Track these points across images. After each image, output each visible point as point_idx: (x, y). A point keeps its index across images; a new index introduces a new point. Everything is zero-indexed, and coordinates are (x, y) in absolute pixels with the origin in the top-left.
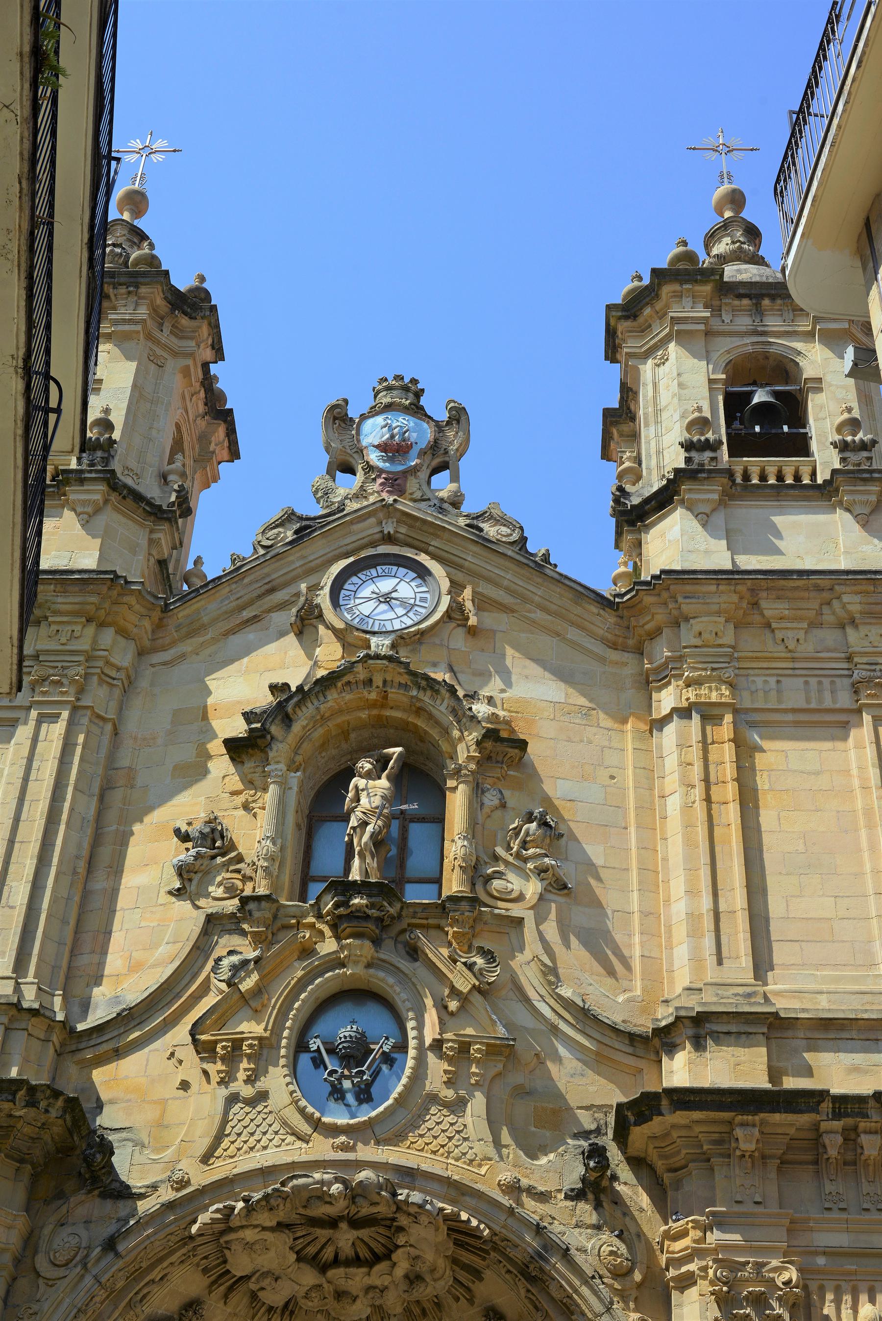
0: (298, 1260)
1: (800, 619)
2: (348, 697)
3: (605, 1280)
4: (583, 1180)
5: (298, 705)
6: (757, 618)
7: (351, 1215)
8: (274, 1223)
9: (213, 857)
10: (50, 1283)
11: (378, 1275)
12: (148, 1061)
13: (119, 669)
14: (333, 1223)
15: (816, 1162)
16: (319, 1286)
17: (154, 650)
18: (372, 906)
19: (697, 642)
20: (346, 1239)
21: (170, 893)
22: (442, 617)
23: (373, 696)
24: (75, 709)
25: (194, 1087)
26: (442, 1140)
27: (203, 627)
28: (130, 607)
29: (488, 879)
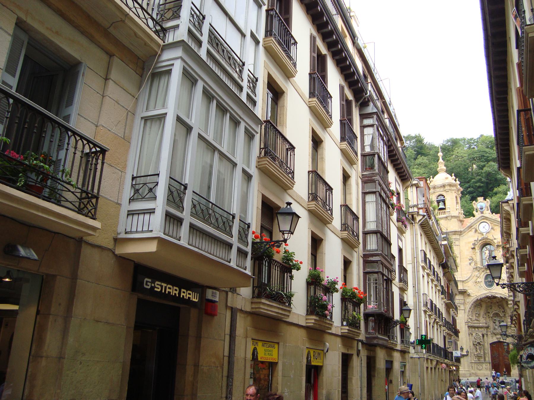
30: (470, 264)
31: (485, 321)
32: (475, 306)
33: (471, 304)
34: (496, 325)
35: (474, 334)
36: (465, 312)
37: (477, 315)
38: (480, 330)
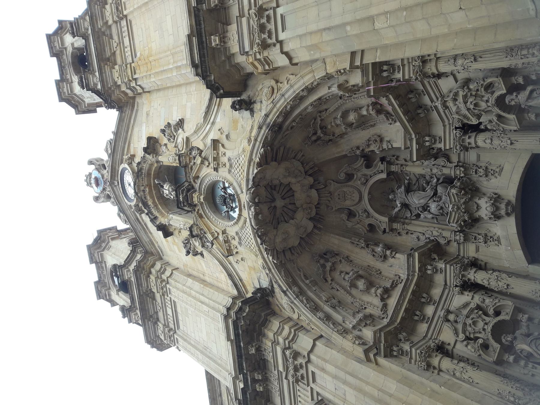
1: (109, 42)
2: (148, 198)
4: (246, 110)
5: (152, 214)
6: (112, 58)
7: (269, 200)
9: (191, 244)
11: (296, 188)
13: (162, 267)
15: (225, 8)
16: (304, 209)
17: (159, 254)
18: (182, 193)
19: (120, 78)
20: (279, 203)
21: (203, 257)
22: (129, 166)
23: (147, 189)
24: (168, 283)
25: (241, 256)
26: (240, 167)
27: (151, 240)
28: (145, 264)
29: (179, 149)
30: (196, 254)
31: (401, 258)
32: (324, 279)
35: (447, 336)
38: (436, 292)
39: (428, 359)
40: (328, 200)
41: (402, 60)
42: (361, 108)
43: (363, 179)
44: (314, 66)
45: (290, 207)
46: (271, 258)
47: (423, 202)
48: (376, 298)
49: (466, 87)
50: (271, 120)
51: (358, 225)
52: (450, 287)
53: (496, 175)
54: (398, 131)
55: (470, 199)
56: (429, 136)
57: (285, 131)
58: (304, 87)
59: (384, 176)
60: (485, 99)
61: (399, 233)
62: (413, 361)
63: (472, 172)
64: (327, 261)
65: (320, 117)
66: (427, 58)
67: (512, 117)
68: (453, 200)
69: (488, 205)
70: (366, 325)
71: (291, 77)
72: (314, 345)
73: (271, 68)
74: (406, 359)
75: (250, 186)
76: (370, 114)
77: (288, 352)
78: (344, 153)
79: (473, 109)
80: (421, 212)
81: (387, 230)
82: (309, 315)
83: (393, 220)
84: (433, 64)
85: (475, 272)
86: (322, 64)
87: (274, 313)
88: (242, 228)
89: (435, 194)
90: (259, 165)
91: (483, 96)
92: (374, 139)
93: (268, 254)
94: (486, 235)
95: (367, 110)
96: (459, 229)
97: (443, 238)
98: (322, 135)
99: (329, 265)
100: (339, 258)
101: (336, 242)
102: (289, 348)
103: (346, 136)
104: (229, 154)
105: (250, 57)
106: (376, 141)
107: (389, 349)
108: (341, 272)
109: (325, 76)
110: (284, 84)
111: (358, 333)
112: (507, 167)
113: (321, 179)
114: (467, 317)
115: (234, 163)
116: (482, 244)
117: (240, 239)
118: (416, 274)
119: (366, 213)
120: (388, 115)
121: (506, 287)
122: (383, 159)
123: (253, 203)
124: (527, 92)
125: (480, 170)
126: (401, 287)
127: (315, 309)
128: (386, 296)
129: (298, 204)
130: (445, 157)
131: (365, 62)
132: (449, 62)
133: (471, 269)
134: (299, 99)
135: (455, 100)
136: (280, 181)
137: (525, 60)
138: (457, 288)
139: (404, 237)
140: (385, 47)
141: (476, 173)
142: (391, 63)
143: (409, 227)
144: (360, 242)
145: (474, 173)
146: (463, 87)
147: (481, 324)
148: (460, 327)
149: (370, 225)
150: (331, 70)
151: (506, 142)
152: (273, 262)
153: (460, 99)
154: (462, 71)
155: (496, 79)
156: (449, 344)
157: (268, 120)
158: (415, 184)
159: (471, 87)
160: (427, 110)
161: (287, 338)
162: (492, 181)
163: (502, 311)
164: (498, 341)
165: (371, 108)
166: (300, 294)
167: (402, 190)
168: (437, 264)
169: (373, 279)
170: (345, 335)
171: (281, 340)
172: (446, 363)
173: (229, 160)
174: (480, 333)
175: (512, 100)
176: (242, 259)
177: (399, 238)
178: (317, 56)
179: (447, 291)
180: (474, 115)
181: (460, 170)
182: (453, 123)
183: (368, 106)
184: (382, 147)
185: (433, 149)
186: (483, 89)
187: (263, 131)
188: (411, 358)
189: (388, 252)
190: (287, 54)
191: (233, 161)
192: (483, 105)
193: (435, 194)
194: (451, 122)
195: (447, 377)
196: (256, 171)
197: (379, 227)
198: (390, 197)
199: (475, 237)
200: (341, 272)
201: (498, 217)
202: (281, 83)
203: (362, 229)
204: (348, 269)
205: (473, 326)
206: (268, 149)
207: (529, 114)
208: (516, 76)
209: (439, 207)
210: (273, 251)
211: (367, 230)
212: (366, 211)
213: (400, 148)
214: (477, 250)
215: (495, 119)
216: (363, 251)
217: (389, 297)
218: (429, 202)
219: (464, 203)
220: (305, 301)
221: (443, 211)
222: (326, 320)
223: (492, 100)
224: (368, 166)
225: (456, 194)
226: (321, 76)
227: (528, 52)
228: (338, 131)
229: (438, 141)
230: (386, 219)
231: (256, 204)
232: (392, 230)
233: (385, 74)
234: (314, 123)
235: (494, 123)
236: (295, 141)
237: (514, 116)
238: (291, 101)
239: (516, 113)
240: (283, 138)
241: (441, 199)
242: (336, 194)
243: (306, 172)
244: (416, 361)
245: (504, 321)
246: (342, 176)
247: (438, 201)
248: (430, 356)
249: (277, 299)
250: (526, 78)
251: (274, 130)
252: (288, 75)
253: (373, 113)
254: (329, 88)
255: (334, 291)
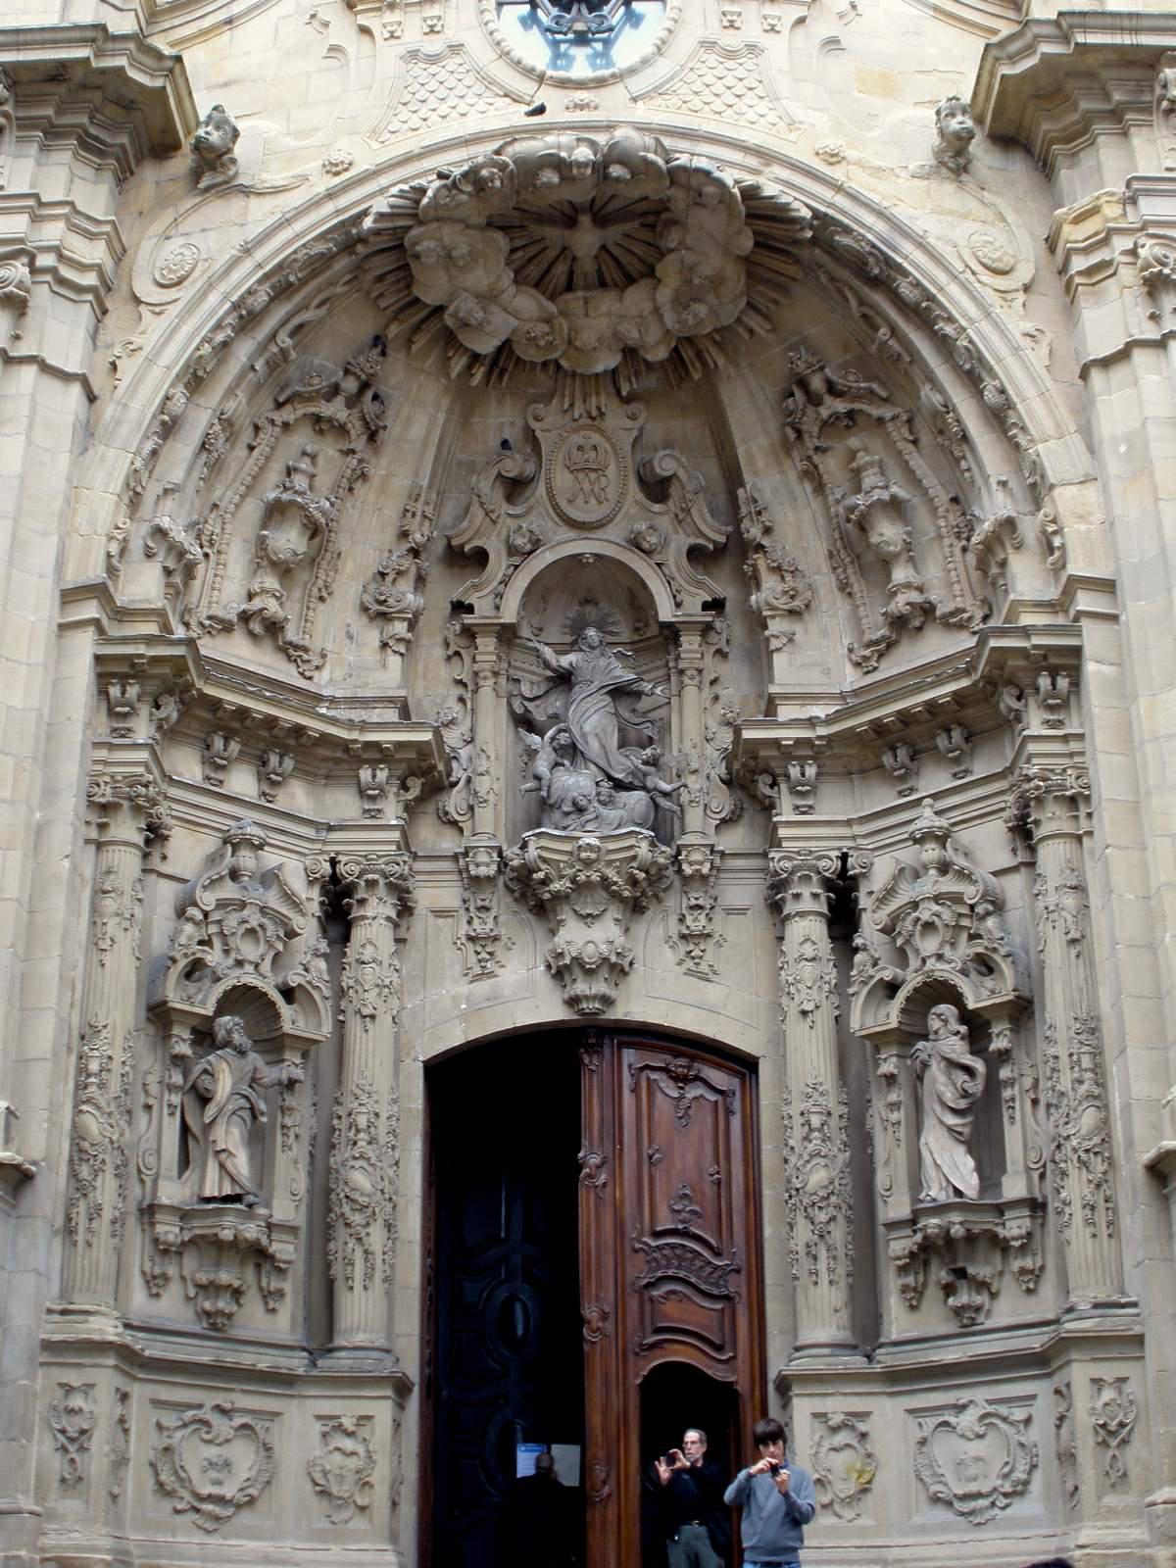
0: (516, 281)
3: (983, 279)
4: (938, 154)
8: (482, 221)
10: (157, 309)
11: (636, 298)
12: (277, 30)
14: (569, 218)
20: (586, 240)
31: (389, 677)
33: (217, 305)
34: (570, 752)
35: (187, 850)
36: (88, 433)
37: (289, 540)
38: (297, 797)
39: (126, 804)
40: (572, 405)
41: (1080, 737)
42: (911, 559)
43: (653, 540)
44: (1076, 441)
45: (561, 269)
46: (381, 205)
47: (593, 748)
48: (244, 593)
49: (991, 908)
50: (906, 258)
51: (481, 514)
52: (324, 842)
53: (690, 964)
54: (827, 672)
55: (616, 896)
56: (818, 774)
57: (856, 294)
58: (1015, 398)
59: (666, 612)
60: (947, 951)
61: (457, 653)
62: (103, 754)
63: (697, 896)
64: (352, 402)
65: (894, 418)
66: (1083, 810)
67: (891, 1015)
68: (611, 846)
69: (604, 948)
70: (168, 572)
71: (1043, 350)
72: (65, 377)
73: (1077, 280)
74: (103, 726)
75: (667, 142)
76: (895, 594)
77: (19, 270)
78: (747, 477)
79: (918, 919)
80: (553, 739)
81: (468, 619)
82: (175, 355)
83: (507, 635)
84: (1067, 827)
85: (388, 919)
86: (1082, 473)
87: (123, 177)
88: (489, 82)
89: (620, 786)
90: (751, 194)
91: (953, 945)
92: (800, 587)
93: (402, 195)
94: (496, 939)
95: (908, 586)
96: (515, 863)
97: (465, 806)
98: (824, 412)
99: (336, 409)
100: (359, 443)
101: (416, 431)
102: (34, 270)
103: (808, 487)
104: (776, 48)
105: (1117, 210)
106: (792, 597)
107: (125, 669)
108: (313, 457)
109: (1043, 476)
110: (1022, 318)
111: (136, 546)
112: (712, 992)
113: (650, 381)
114: (263, 910)
115: (740, 72)
116: (464, 929)
117: (433, 59)
118: (354, 735)
119: (528, 547)
120: (886, 647)
121: (366, 1011)
122: (716, 605)
123: (604, 156)
124: (968, 1060)
125: (702, 918)
126: (287, 673)
127: (195, 379)
128: (256, 627)
129: (574, 300)
130: (733, 812)
131: (1086, 624)
132: (1068, 872)
133: (395, 905)
134: (973, 375)
135: (944, 868)
136: (671, 251)
137: (1064, 1061)
138: (327, 867)
139: (445, 673)
140: (1124, 692)
141: (692, 908)
142: (1073, 699)
143: (486, 691)
144: (421, 525)
145: (693, 902)
146: (987, 896)
147: (250, 951)
148: (229, 891)
149: (480, 558)
150: (1065, 500)
151: (806, 999)
152: (365, 213)
153: (948, 885)
154: (1041, 905)
155: (1010, 987)
156: (164, 858)
157: (908, 247)
158: (634, 711)
159: (991, 922)
160: (903, 778)
161: (61, 257)
162: (668, 953)
163: (295, 1006)
164: (226, 1005)
165: (915, 597)
166: (241, 317)
167: (618, 672)
168: (392, 797)
169: (303, 576)
170: (126, 500)
171: (53, 232)
172: (128, 862)
173: (752, 48)
174: (227, 952)
175: (946, 1022)
176: (333, 48)
177: (439, 652)
178: (1114, 466)
179: (309, 832)
180: (895, 918)
181: (701, 863)
182: (856, 848)
183: (920, 589)
184: (773, 617)
185: (774, 784)
186: (980, 950)
187: (869, 219)
188: (111, 747)
189: (400, 628)
190: (1123, 355)
191: (749, 64)
192: (929, 945)
193: (620, 786)
194: (859, 841)
195: (88, 870)
196: (728, 177)
197: (476, 587)
198: (591, 632)
199: (487, 909)
200: (313, 457)
201: (560, 974)
202: (1024, 305)
203: (469, 527)
204: (324, 481)
205: (242, 930)
206: (802, 229)
207: (894, 1059)
208: (1011, 1030)
209: (584, 803)
210: (412, 212)
211: (462, 546)
212: (537, 544)
213: (771, 680)
214: (439, 913)
215: (887, 975)
216: (390, 534)
217: (252, 635)
218: (592, 767)
219: (604, 879)
220: (220, 337)
221: (567, 814)
222: (163, 423)
223: (944, 971)
224: (695, 554)
225: (634, 858)
226: (1046, 464)
227: (1086, 1070)
228: (831, 466)
229: (800, 802)
230: (509, 614)
231: (600, 167)
232: (469, 633)
233: (1044, 682)
234: (872, 392)
235: (871, 972)
236: (809, 316)
237: (894, 1023)
238: (971, 341)
239: (903, 1027)
240: (833, 279)
241: (603, 803)
242: (596, 438)
243: (689, 340)
244: (105, 763)
245: (277, 1016)
246: (665, 466)
247: (598, 794)
248: (137, 809)
249: (195, 207)
250: (1004, 1056)
251: (871, 260)
252: (1049, 336)
253: (900, 603)
254: (1003, 484)
255: (247, 436)
